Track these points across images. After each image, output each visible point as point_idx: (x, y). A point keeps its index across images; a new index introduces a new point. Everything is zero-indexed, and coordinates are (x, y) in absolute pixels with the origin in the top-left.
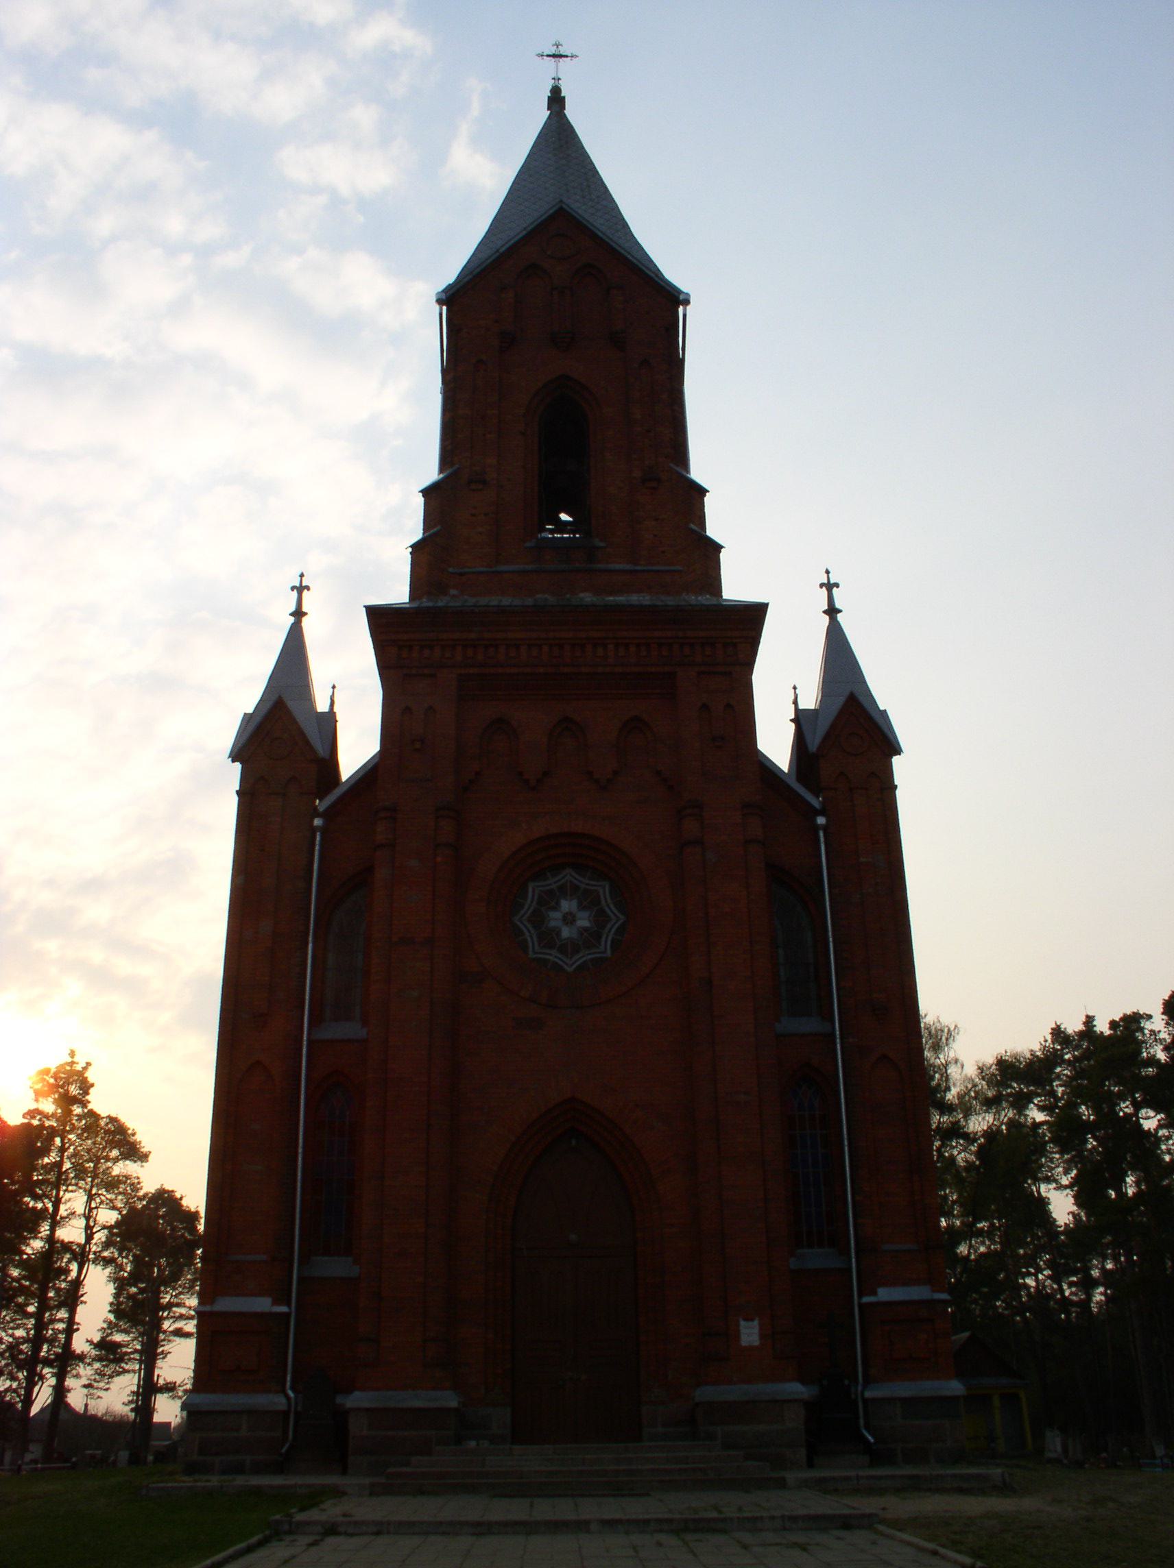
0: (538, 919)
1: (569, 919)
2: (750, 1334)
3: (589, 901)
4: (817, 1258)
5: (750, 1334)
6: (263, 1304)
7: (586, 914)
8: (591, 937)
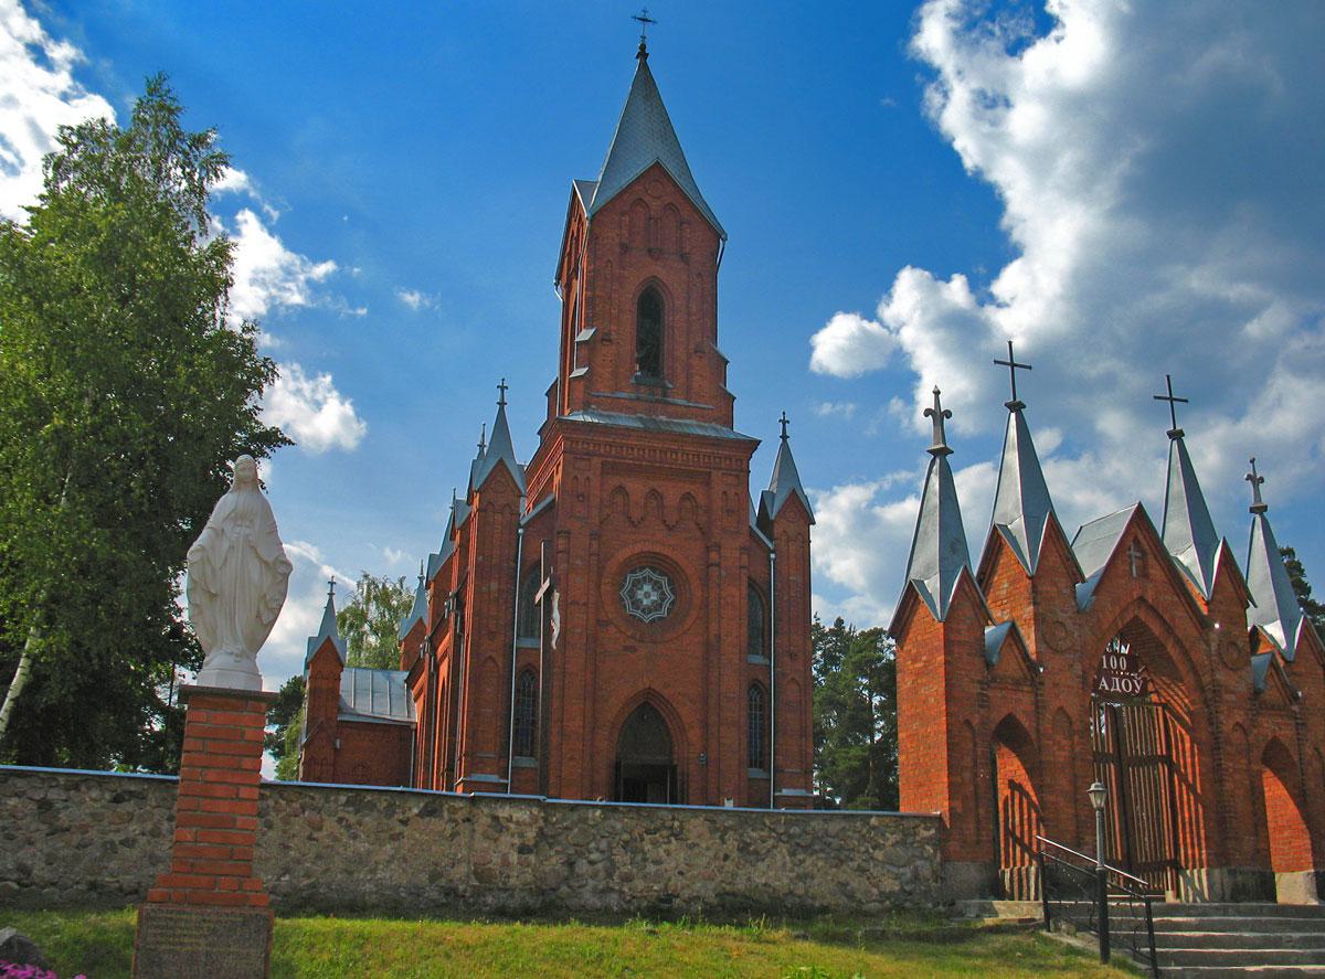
0: (632, 594)
1: (647, 595)
3: (657, 586)
4: (756, 773)
7: (655, 593)
8: (657, 606)
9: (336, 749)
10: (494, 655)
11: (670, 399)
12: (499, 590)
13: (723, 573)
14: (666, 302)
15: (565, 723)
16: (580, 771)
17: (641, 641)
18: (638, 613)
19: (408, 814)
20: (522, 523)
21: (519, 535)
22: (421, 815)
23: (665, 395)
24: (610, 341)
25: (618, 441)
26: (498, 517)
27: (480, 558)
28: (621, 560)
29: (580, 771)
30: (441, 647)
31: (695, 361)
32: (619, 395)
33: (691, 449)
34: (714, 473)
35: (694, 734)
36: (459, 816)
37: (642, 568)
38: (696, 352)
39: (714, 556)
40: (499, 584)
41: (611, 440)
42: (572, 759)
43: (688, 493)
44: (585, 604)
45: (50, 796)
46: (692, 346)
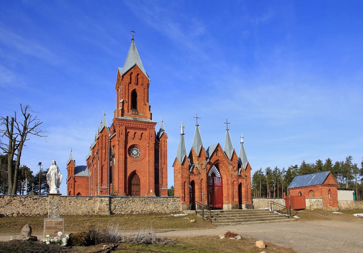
11: (139, 114)
13: (150, 148)
18: (133, 156)
19: (86, 200)
22: (89, 200)
23: (138, 113)
36: (96, 200)
45: (21, 199)
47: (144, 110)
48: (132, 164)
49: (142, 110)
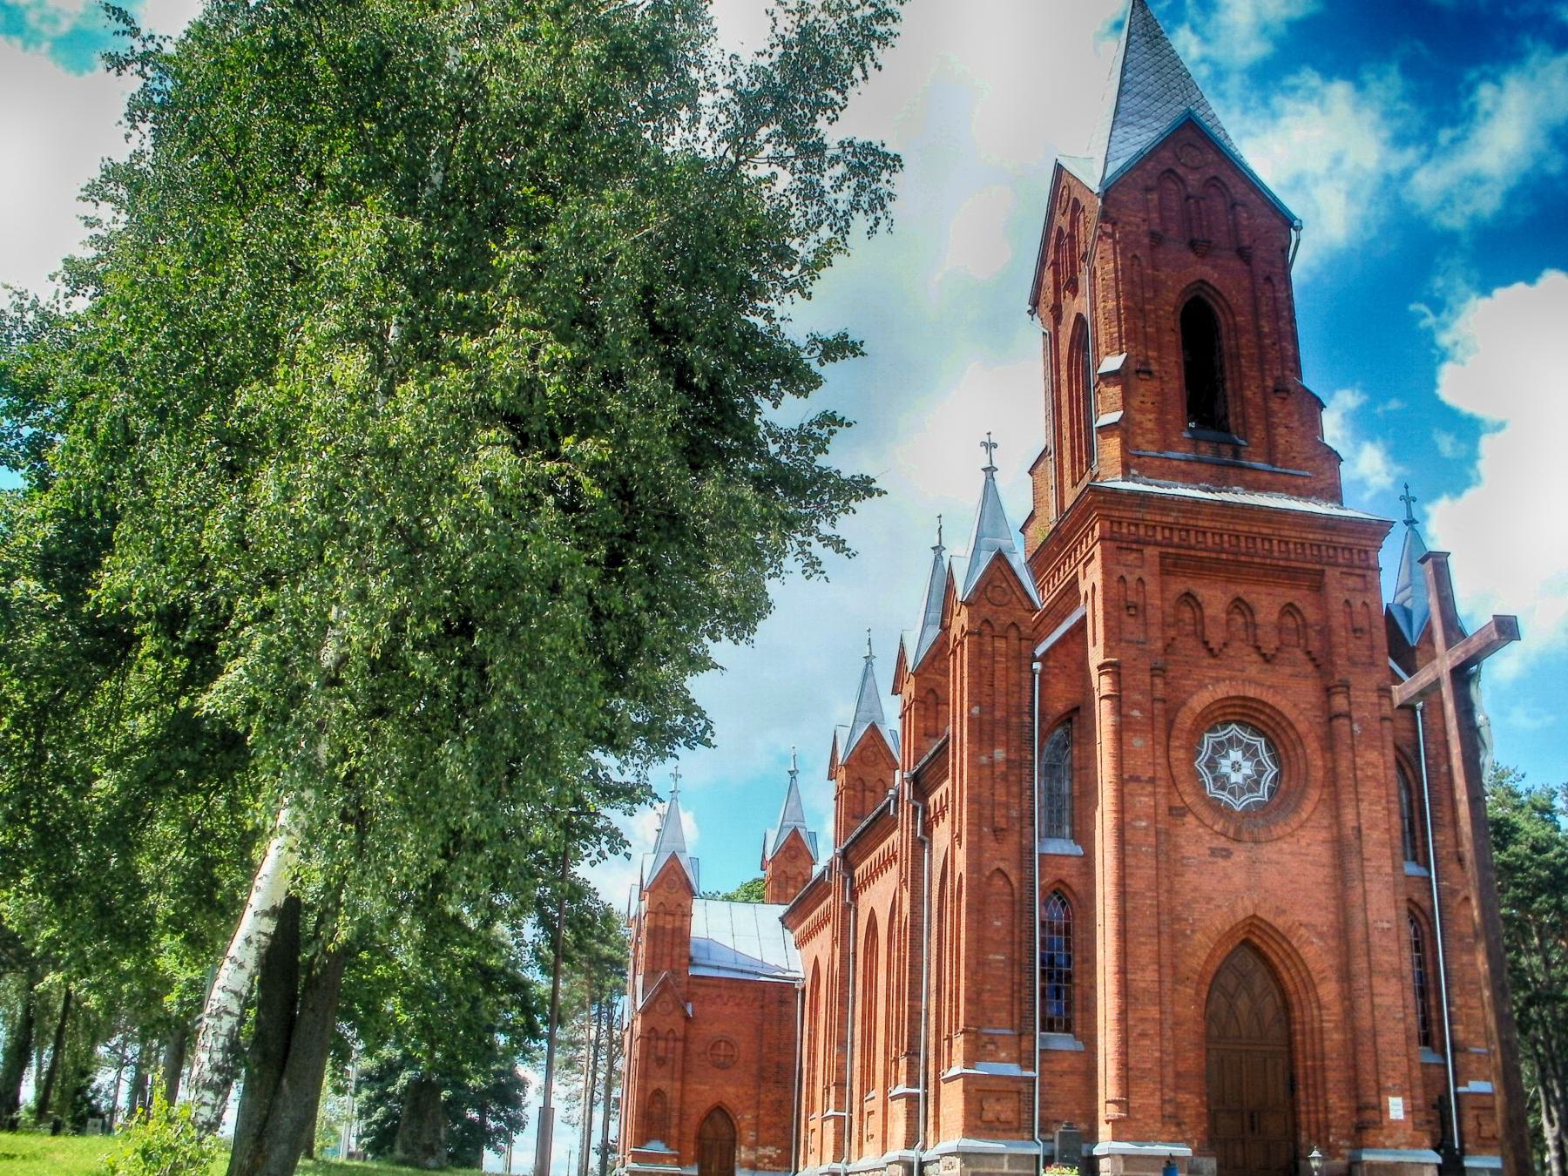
0: (1212, 765)
1: (1236, 767)
2: (1396, 1108)
3: (1251, 753)
5: (1396, 1108)
6: (1013, 1070)
8: (1253, 784)
9: (687, 1018)
10: (1002, 865)
12: (1008, 761)
13: (1356, 727)
14: (1222, 319)
15: (1130, 976)
16: (1157, 1054)
17: (1238, 840)
20: (1039, 651)
21: (1033, 672)
23: (1236, 455)
24: (1150, 373)
25: (1182, 521)
26: (1000, 644)
27: (976, 710)
28: (1198, 710)
29: (1157, 1054)
30: (863, 866)
31: (1275, 405)
32: (1171, 454)
33: (1293, 534)
34: (1329, 571)
35: (1329, 991)
37: (1227, 723)
38: (1276, 391)
39: (1340, 702)
40: (1008, 751)
41: (1171, 520)
42: (1143, 1035)
43: (1290, 604)
44: (1152, 780)
46: (1270, 383)
47: (1282, 430)
48: (1221, 862)
49: (1259, 433)
